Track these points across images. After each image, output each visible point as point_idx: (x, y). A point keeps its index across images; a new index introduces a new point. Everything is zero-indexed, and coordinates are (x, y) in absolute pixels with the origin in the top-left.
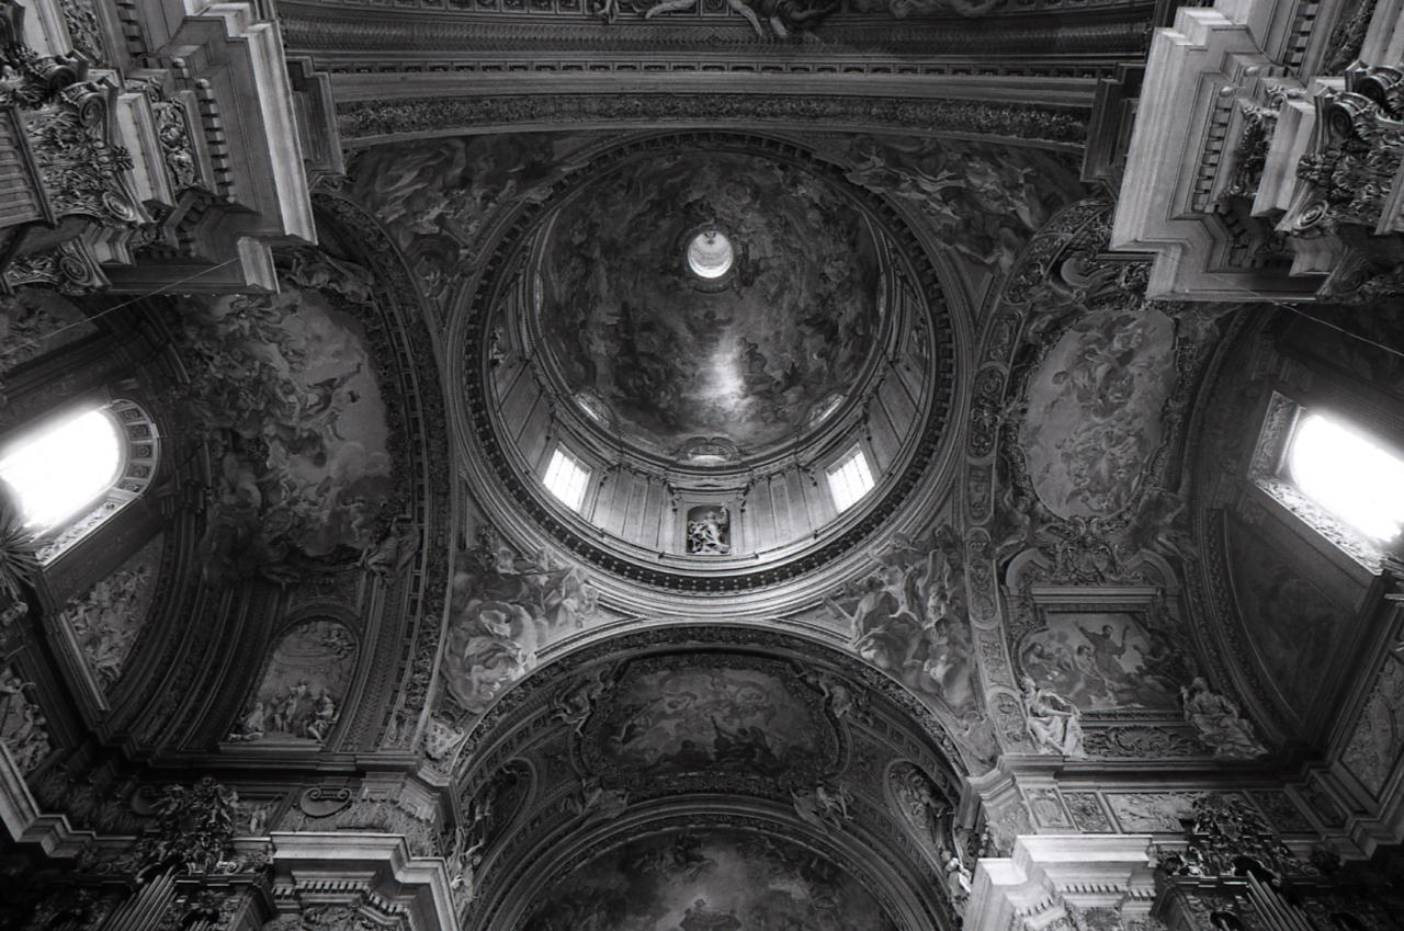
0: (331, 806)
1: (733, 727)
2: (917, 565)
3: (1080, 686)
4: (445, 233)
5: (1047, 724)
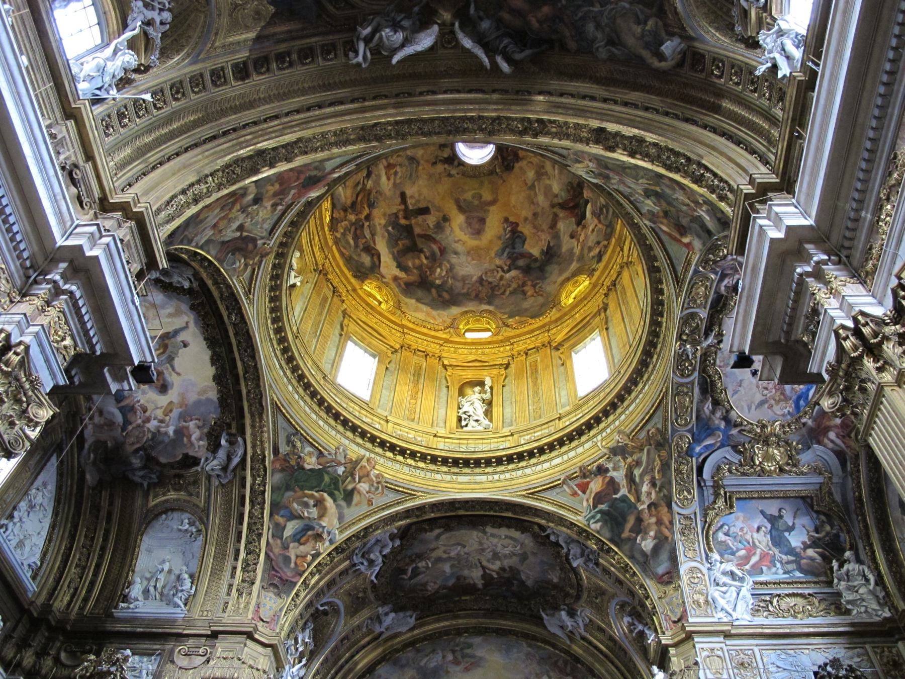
0: (199, 660)
1: (496, 566)
2: (635, 457)
3: (754, 559)
4: (245, 234)
5: (725, 593)
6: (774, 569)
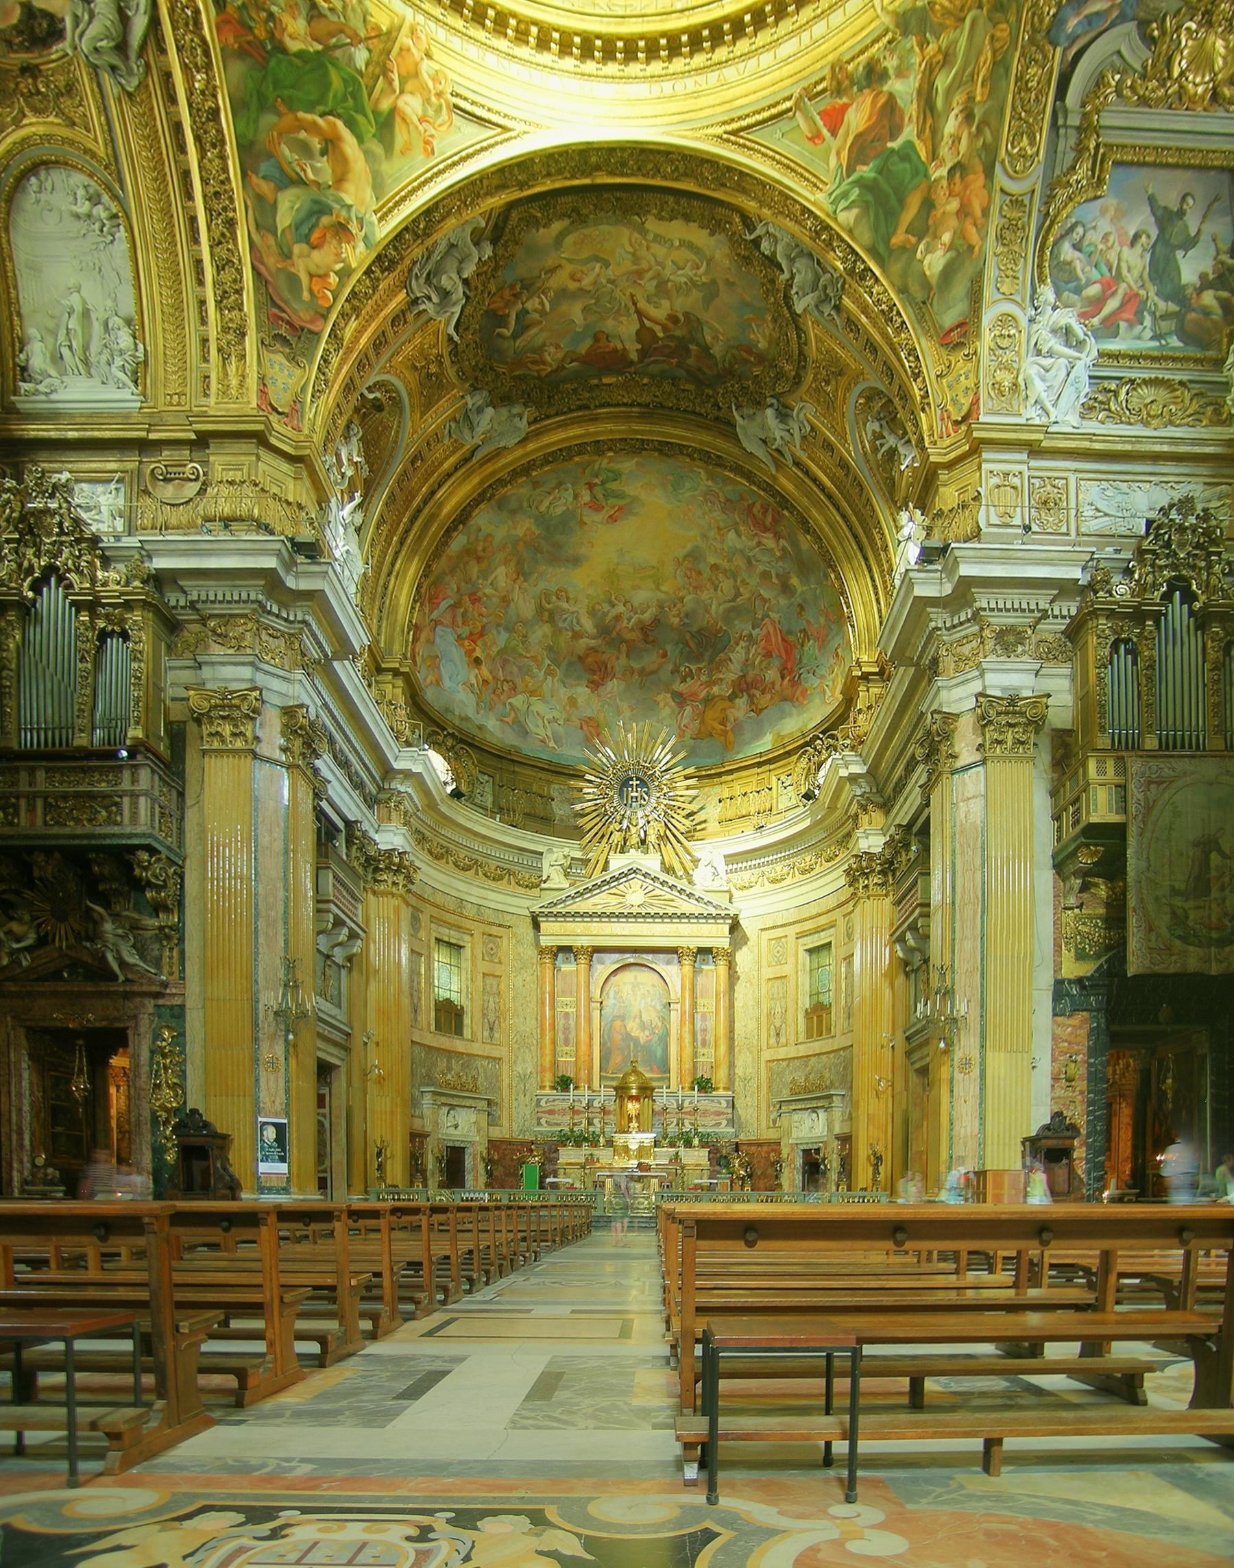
6: (1140, 328)
